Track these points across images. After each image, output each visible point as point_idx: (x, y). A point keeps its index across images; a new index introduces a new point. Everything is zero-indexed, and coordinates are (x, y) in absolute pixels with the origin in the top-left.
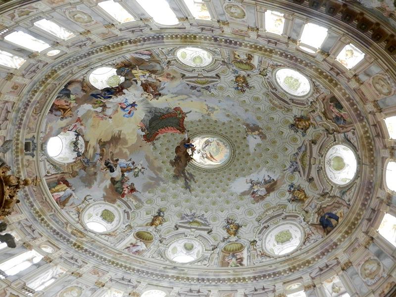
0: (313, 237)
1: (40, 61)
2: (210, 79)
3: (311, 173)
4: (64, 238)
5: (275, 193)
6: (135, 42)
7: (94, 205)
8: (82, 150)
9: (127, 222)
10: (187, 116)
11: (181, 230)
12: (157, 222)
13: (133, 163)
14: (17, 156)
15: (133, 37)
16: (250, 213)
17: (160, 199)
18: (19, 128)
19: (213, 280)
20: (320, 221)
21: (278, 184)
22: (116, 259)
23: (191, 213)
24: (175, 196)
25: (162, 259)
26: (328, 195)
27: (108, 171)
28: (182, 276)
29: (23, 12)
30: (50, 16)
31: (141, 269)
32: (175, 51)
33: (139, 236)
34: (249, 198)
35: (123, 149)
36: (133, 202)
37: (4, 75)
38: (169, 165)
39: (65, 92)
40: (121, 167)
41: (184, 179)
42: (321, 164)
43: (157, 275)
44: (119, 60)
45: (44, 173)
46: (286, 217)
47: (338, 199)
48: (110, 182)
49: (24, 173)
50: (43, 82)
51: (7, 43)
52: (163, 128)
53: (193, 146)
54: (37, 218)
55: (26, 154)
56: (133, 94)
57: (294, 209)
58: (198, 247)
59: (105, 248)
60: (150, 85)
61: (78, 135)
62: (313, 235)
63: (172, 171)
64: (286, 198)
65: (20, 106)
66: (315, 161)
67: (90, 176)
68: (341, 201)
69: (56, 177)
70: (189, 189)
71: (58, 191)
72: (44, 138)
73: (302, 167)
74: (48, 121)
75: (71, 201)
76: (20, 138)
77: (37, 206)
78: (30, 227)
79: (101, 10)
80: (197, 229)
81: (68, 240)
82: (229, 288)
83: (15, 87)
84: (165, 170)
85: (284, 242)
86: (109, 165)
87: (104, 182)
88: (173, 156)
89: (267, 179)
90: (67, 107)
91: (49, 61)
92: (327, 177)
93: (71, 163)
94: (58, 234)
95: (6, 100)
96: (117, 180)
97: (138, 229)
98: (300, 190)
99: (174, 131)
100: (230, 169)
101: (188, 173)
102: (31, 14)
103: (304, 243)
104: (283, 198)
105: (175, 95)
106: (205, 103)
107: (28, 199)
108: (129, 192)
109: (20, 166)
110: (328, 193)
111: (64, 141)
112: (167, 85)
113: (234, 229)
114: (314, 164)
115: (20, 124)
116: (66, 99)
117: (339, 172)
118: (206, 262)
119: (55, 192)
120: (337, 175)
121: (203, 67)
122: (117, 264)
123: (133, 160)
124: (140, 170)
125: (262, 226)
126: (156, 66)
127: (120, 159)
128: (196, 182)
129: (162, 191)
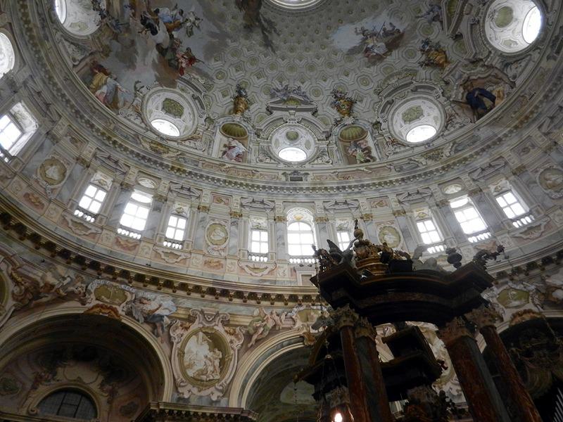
0: (458, 120)
3: (461, 26)
4: (155, 162)
5: (400, 53)
7: (150, 96)
9: (204, 113)
11: (276, 114)
12: (242, 106)
13: (181, 13)
16: (365, 80)
19: (356, 187)
20: (467, 98)
21: (405, 36)
24: (253, 61)
26: (481, 63)
27: (149, 33)
28: (319, 186)
34: (360, 56)
40: (165, 23)
41: (260, 30)
42: (480, 15)
46: (417, 88)
47: (496, 71)
48: (157, 53)
49: (58, 78)
57: (428, 77)
58: (305, 135)
62: (457, 117)
64: (417, 59)
66: (471, 10)
68: (500, 75)
69: (87, 64)
70: (272, 47)
71: (99, 87)
73: (447, 16)
81: (161, 165)
82: (377, 194)
84: (230, 17)
85: (414, 120)
86: (147, 22)
87: (149, 53)
89: (389, 28)
92: (485, 36)
93: (95, 33)
94: (144, 158)
96: (165, 46)
97: (221, 121)
98: (439, 50)
100: (329, 10)
101: (265, 20)
103: (446, 127)
104: (411, 61)
107: (82, 117)
110: (482, 60)
113: (346, 107)
114: (467, 14)
117: (502, 29)
118: (327, 158)
120: (498, 34)
122: (236, 183)
123: (180, 7)
124: (194, 23)
125: (384, 101)
127: (160, 9)
128: (279, 35)
129: (233, 55)
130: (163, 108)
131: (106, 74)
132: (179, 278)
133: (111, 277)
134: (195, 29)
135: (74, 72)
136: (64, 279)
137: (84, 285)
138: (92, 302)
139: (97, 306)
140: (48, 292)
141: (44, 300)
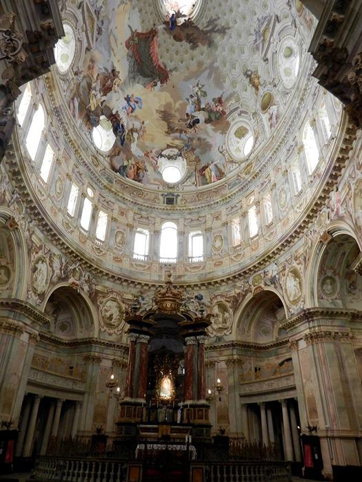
1: (99, 200)
2: (86, 14)
6: (66, 131)
8: (176, 151)
10: (136, 30)
11: (269, 56)
12: (256, 81)
13: (192, 96)
14: (177, 210)
15: (61, 134)
17: (233, 70)
18: (154, 208)
22: (273, 149)
23: (253, 35)
24: (232, 50)
25: (289, 95)
27: (197, 125)
31: (286, 130)
32: (63, 76)
33: (265, 107)
35: (176, 108)
36: (231, 104)
38: (196, 52)
39: (122, 171)
40: (195, 111)
41: (213, 34)
43: (295, 118)
44: (85, 128)
45: (193, 188)
48: (209, 124)
50: (115, 194)
52: (151, 60)
53: (173, 15)
54: (227, 201)
55: (176, 202)
56: (117, 102)
58: (290, 42)
59: (266, 149)
60: (104, 85)
61: (162, 156)
63: (202, 48)
67: (200, 145)
71: (210, 177)
72: (163, 186)
74: (148, 186)
75: (221, 167)
76: (162, 208)
77: (218, 199)
78: (232, 208)
79: (49, 178)
80: (272, 35)
81: (249, 182)
83: (122, 214)
88: (185, 45)
90: (136, 167)
91: (97, 193)
94: (242, 188)
95: (132, 218)
97: (259, 107)
99: (155, 44)
101: (207, 26)
105: (112, 52)
106: (116, 10)
108: (222, 106)
109: (185, 208)
111: (166, 166)
112: (101, 66)
116: (128, 169)
119: (211, 180)
121: (73, 30)
122: (277, 149)
123: (188, 97)
124: (200, 88)
126: (83, 86)
128: (219, 18)
129: (225, 66)
130: (240, 138)
131: (207, 167)
134: (203, 89)
135: (199, 188)
139: (256, 289)
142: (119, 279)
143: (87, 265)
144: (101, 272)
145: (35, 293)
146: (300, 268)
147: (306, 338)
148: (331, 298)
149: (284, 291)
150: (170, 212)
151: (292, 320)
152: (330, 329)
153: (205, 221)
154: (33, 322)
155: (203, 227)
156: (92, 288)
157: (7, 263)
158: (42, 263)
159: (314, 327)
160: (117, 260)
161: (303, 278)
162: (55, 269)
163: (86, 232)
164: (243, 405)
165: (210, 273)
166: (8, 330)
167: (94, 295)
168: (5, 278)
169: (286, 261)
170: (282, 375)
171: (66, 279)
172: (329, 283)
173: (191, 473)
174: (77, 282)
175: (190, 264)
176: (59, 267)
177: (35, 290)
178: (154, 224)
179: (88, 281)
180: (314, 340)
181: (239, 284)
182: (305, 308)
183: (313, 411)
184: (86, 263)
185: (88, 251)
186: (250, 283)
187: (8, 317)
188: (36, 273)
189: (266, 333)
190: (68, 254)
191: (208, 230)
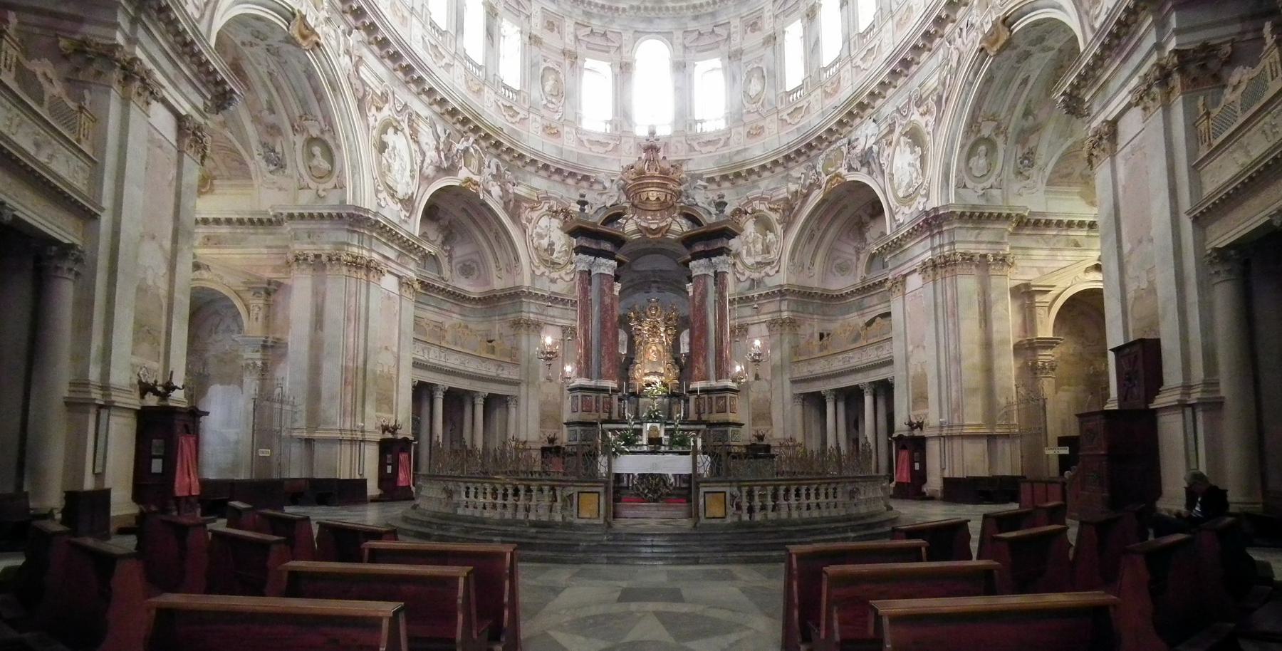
14: (667, 9)
18: (617, 9)
29: (436, 55)
30: (422, 10)
37: (535, 49)
51: (486, 59)
65: (581, 12)
83: (550, 26)
95: (573, 38)
102: (433, 42)
115: (610, 8)
132: (862, 92)
133: (826, 143)
136: (800, 178)
137: (814, 171)
138: (824, 179)
140: (796, 200)
141: (797, 208)
142: (559, 171)
143: (493, 143)
144: (521, 156)
145: (393, 196)
146: (925, 122)
147: (924, 268)
148: (981, 186)
149: (887, 179)
150: (653, 14)
151: (899, 235)
152: (972, 248)
153: (729, 36)
154: (400, 255)
155: (724, 48)
156: (507, 191)
157: (322, 132)
158: (396, 133)
159: (941, 246)
160: (552, 131)
161: (930, 145)
162: (425, 148)
163: (480, 68)
164: (795, 397)
165: (738, 152)
166: (354, 269)
167: (514, 206)
168: (325, 165)
169: (898, 110)
170: (870, 341)
171: (451, 170)
172: (983, 153)
173: (701, 501)
174: (476, 178)
175: (697, 137)
176: (433, 143)
177: (392, 193)
178: (619, 48)
179: (497, 177)
180: (939, 271)
181: (796, 173)
182: (927, 209)
183: (920, 398)
184: (487, 137)
185: (489, 110)
186: (819, 168)
187: (348, 244)
188: (386, 155)
189: (844, 269)
190: (447, 117)
191: (735, 56)
